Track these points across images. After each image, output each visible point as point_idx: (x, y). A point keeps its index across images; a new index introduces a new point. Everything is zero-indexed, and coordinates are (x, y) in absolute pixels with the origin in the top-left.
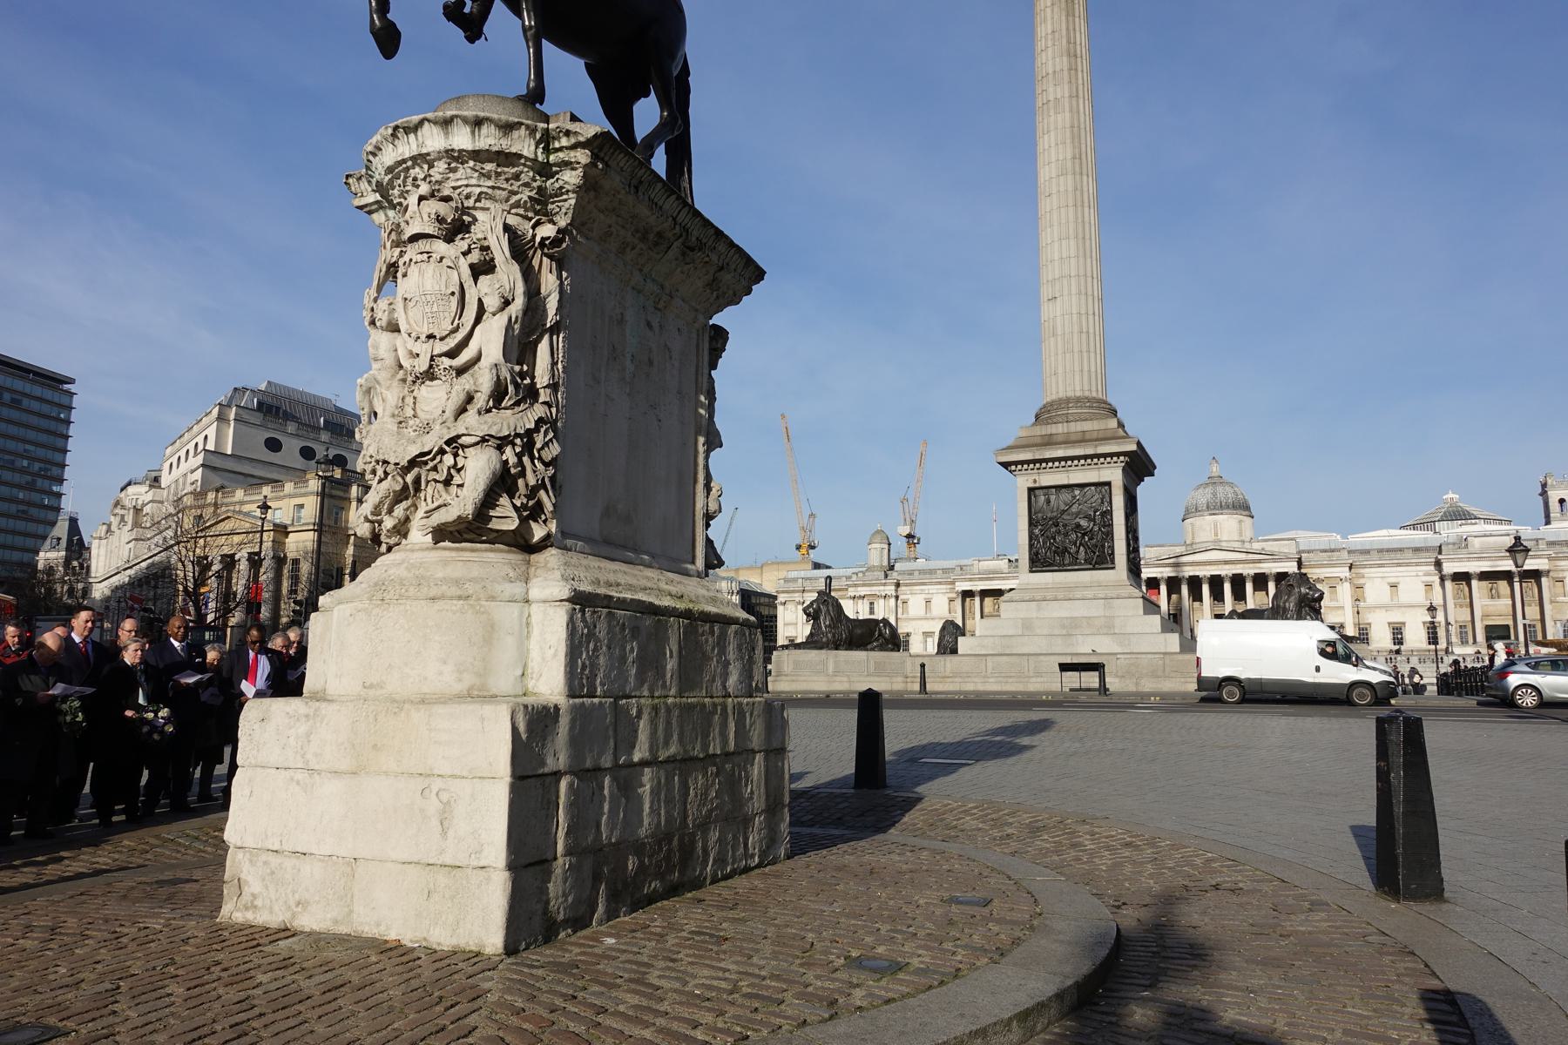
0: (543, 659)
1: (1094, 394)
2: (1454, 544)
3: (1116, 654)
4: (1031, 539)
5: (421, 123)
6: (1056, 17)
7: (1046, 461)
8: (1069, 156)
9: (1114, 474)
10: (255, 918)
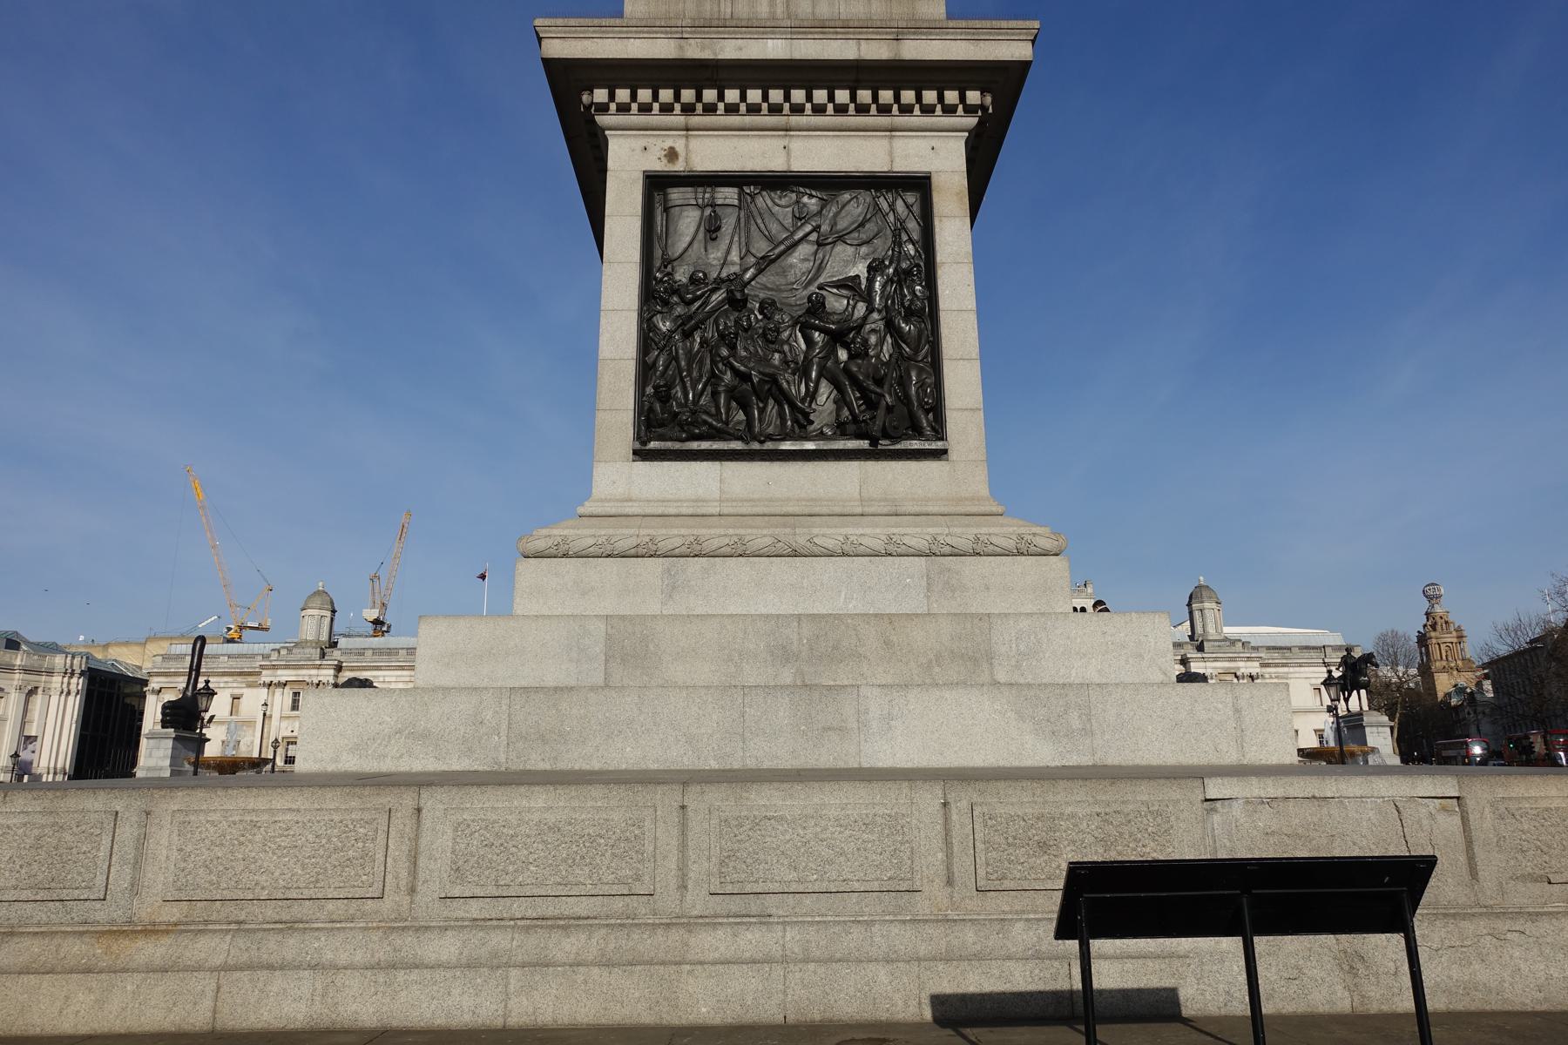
3: (1199, 774)
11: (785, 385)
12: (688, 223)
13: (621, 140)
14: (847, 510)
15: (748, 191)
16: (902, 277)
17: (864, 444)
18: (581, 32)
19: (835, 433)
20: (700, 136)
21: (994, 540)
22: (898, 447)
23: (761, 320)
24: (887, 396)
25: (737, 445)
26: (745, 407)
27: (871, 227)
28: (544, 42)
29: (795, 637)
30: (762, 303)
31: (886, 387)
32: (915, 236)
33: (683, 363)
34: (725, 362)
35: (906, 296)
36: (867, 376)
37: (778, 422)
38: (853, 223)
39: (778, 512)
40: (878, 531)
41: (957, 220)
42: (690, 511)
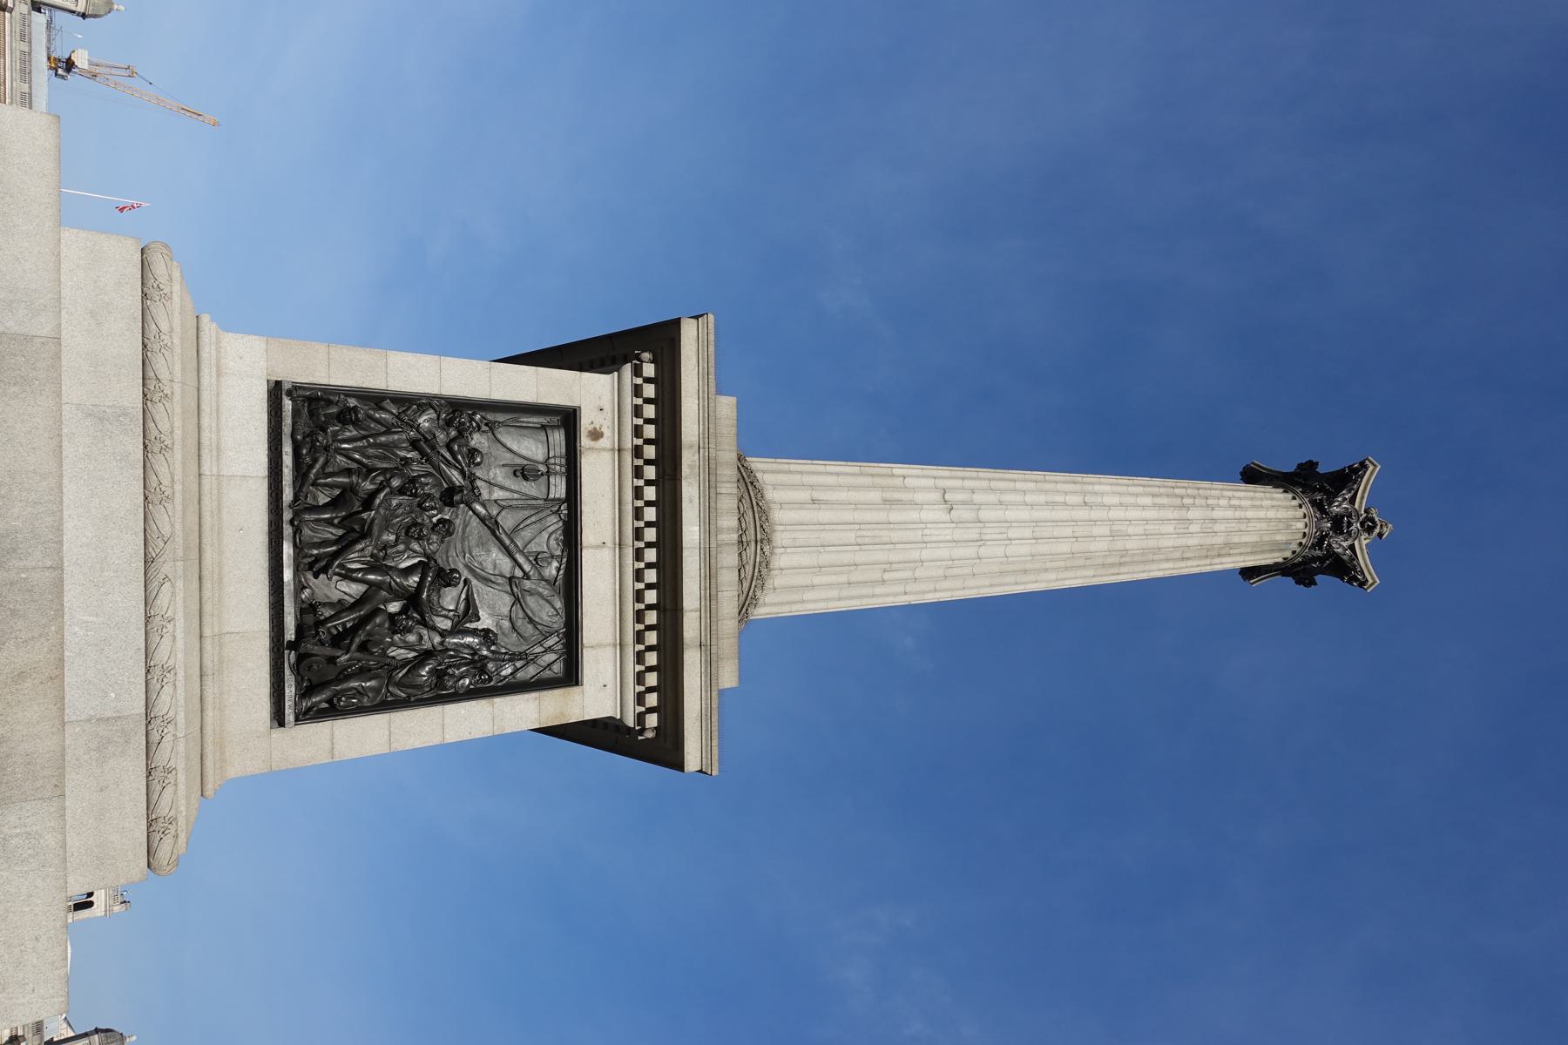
11: (359, 547)
12: (531, 448)
13: (608, 387)
14: (207, 619)
15: (562, 508)
16: (478, 664)
17: (290, 634)
18: (703, 355)
19: (303, 602)
20: (614, 462)
21: (169, 791)
22: (287, 671)
23: (431, 521)
24: (346, 657)
25: (288, 495)
26: (333, 504)
27: (529, 630)
28: (694, 321)
29: (30, 563)
30: (449, 521)
31: (358, 655)
32: (520, 675)
33: (383, 439)
34: (385, 483)
35: (458, 669)
36: (369, 634)
37: (315, 540)
38: (532, 612)
39: (204, 540)
40: (180, 656)
41: (536, 716)
42: (205, 441)
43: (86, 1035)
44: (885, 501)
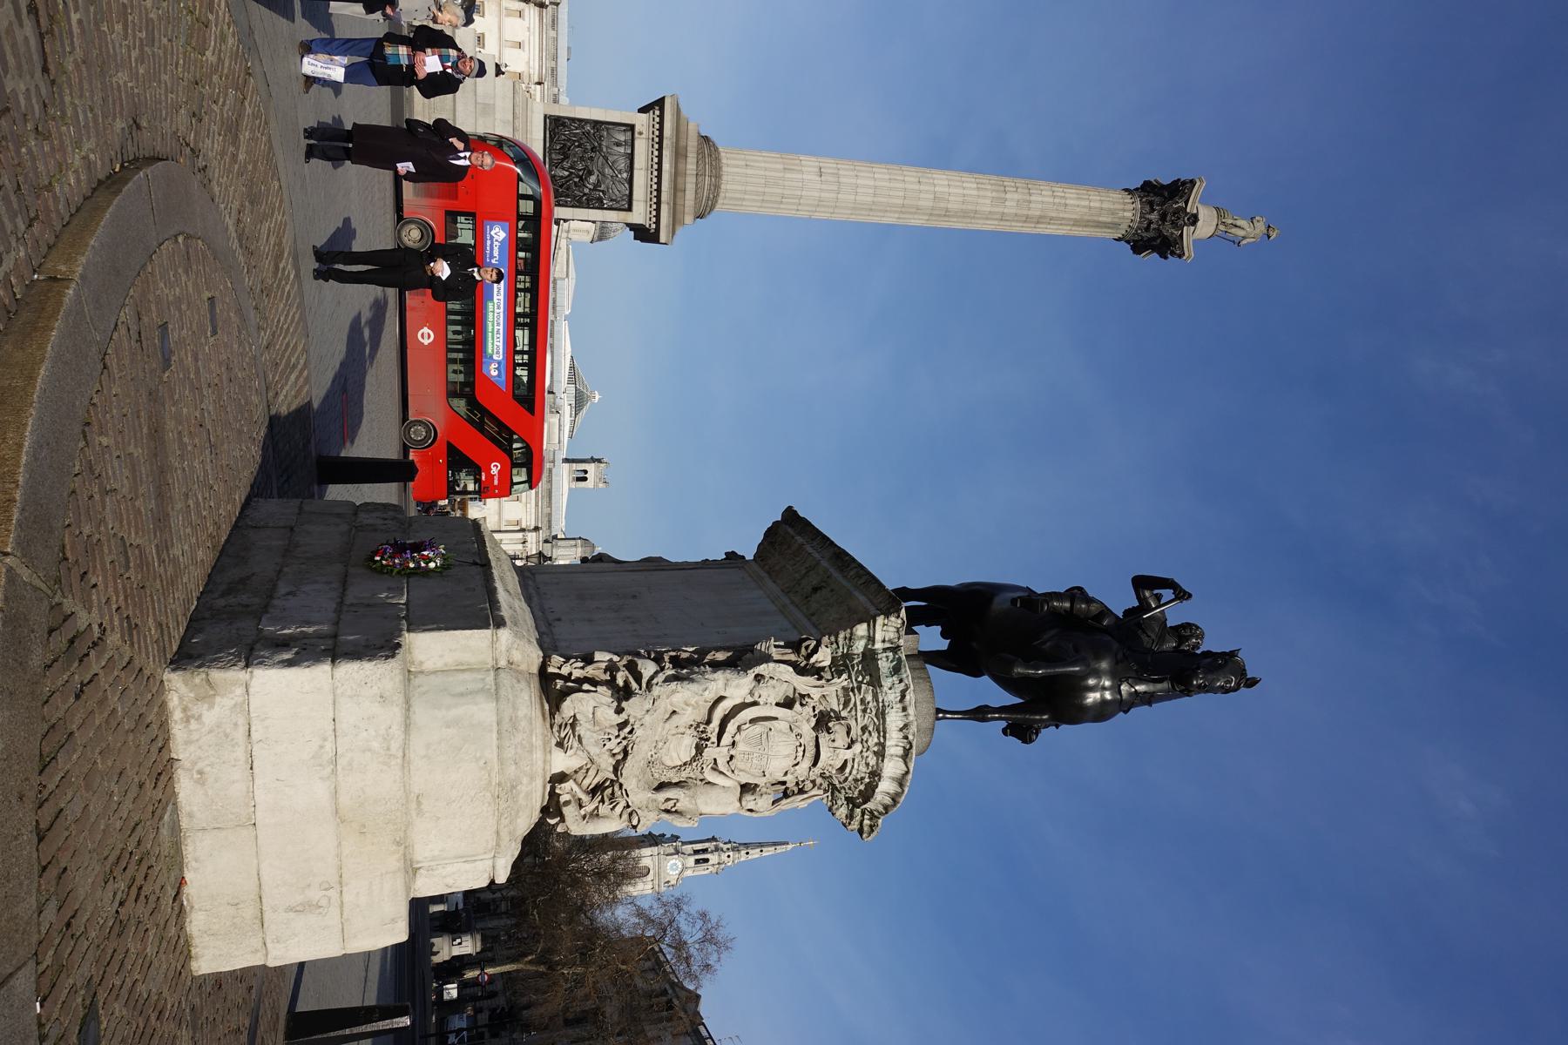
0: (445, 877)
1: (720, 201)
2: (554, 404)
4: (581, 120)
5: (907, 767)
6: (1078, 209)
7: (660, 150)
8: (950, 206)
9: (640, 215)
10: (176, 722)
12: (622, 137)
25: (548, 145)
43: (574, 539)
44: (785, 169)
